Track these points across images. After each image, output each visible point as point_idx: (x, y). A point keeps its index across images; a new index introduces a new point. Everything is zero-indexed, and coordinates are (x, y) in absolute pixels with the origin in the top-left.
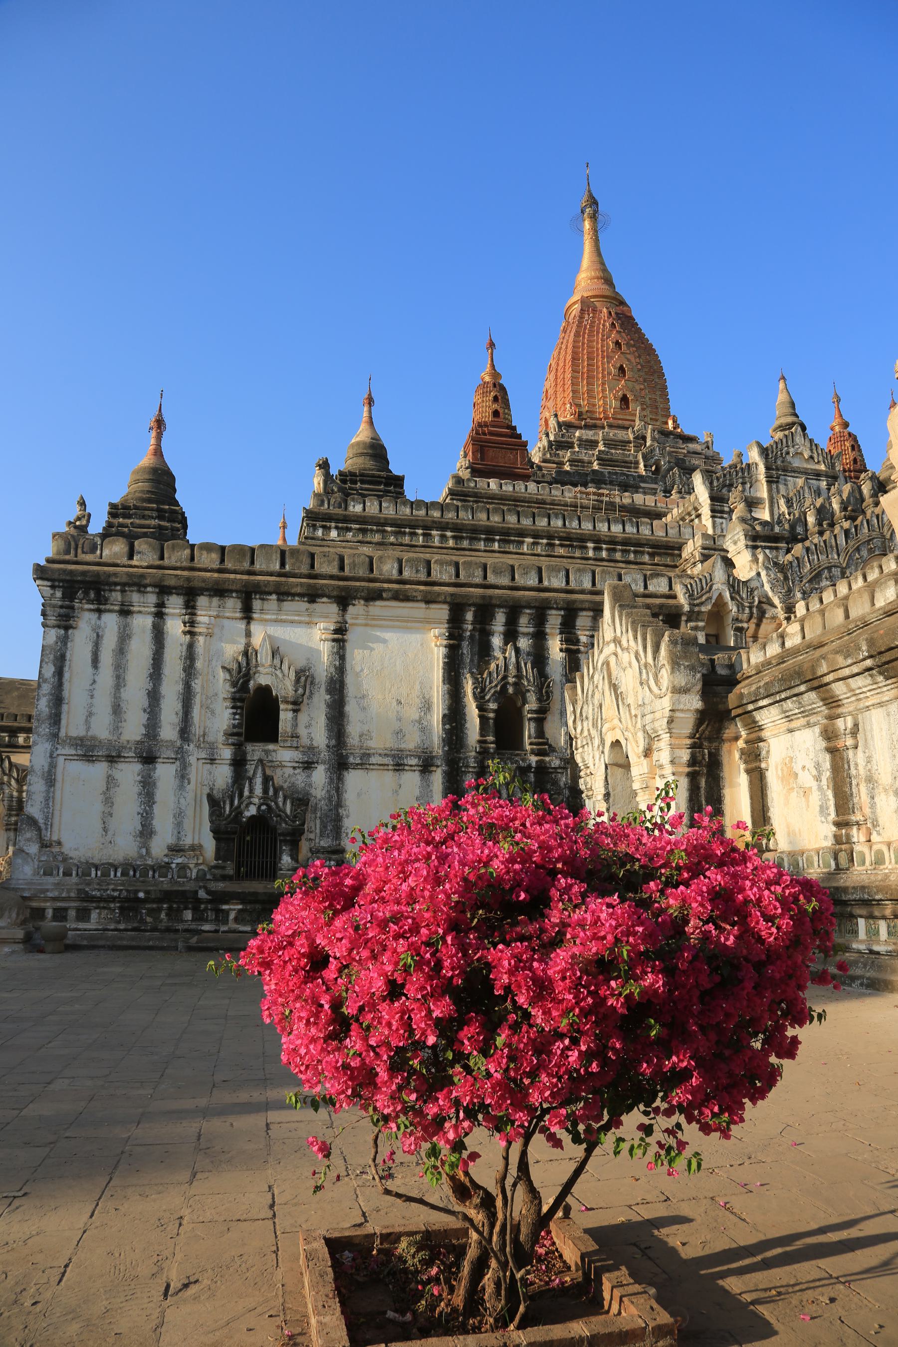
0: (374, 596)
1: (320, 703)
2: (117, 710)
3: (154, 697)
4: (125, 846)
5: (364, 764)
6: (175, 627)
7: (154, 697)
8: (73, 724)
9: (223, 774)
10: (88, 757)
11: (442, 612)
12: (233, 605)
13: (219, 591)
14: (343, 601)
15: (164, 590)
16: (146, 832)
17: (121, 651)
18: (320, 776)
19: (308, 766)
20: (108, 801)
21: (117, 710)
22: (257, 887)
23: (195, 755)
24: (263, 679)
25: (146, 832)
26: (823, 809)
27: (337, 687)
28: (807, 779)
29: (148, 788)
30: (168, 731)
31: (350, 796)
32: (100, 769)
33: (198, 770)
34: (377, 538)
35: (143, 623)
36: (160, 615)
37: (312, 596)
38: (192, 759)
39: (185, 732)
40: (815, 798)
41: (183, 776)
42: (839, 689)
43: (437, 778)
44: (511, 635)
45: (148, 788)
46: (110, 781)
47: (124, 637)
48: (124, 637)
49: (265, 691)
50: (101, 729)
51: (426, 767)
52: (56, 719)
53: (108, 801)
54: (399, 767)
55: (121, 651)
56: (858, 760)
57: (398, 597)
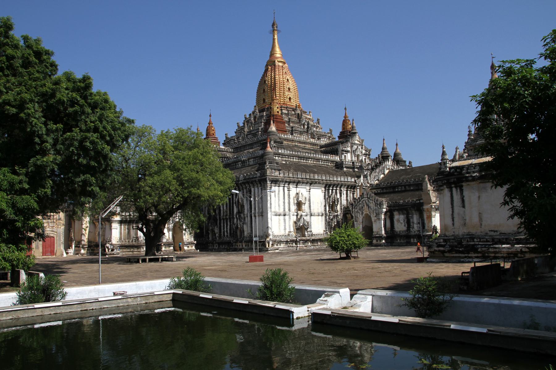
0: (316, 183)
1: (307, 203)
2: (279, 206)
3: (284, 202)
4: (282, 233)
5: (314, 215)
6: (286, 188)
7: (284, 202)
8: (273, 210)
9: (295, 217)
10: (276, 215)
11: (324, 186)
12: (295, 184)
13: (294, 182)
14: (311, 184)
15: (286, 182)
16: (285, 229)
17: (279, 194)
18: (309, 216)
19: (306, 215)
20: (279, 223)
21: (279, 206)
22: (304, 238)
23: (291, 214)
24: (300, 199)
25: (285, 229)
26: (405, 226)
27: (309, 200)
28: (402, 221)
29: (285, 220)
30: (287, 210)
31: (312, 221)
32: (278, 217)
33: (292, 217)
34: (285, 159)
35: (281, 188)
36: (284, 187)
37: (307, 183)
38: (291, 215)
39: (289, 210)
40: (403, 224)
41: (290, 218)
42: (410, 211)
43: (324, 217)
44: (332, 190)
45: (285, 220)
46: (279, 220)
47: (279, 191)
48: (279, 191)
49: (301, 201)
50: (277, 210)
51: (322, 215)
52: (271, 207)
53: (279, 223)
54: (319, 215)
55: (279, 194)
56: (411, 220)
57: (319, 183)
